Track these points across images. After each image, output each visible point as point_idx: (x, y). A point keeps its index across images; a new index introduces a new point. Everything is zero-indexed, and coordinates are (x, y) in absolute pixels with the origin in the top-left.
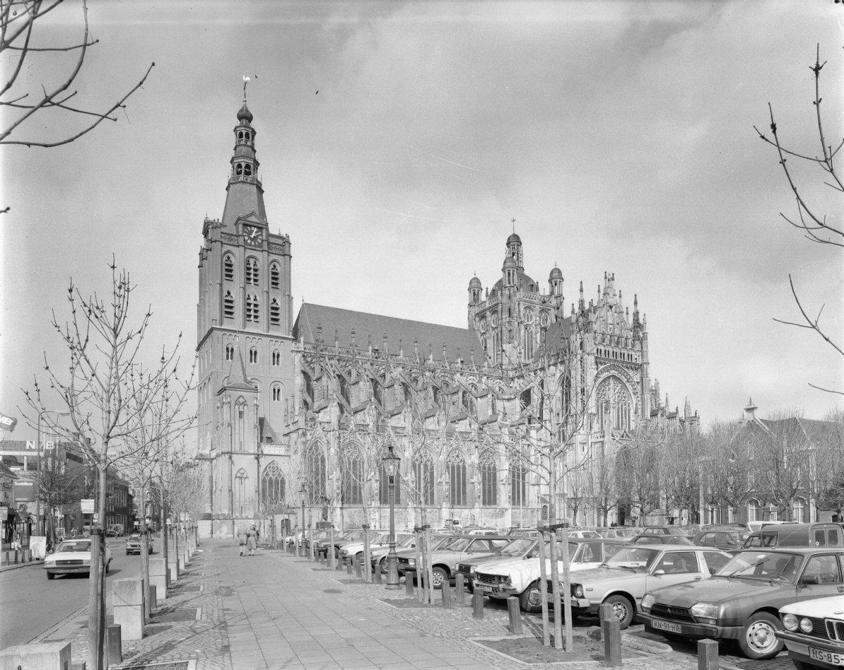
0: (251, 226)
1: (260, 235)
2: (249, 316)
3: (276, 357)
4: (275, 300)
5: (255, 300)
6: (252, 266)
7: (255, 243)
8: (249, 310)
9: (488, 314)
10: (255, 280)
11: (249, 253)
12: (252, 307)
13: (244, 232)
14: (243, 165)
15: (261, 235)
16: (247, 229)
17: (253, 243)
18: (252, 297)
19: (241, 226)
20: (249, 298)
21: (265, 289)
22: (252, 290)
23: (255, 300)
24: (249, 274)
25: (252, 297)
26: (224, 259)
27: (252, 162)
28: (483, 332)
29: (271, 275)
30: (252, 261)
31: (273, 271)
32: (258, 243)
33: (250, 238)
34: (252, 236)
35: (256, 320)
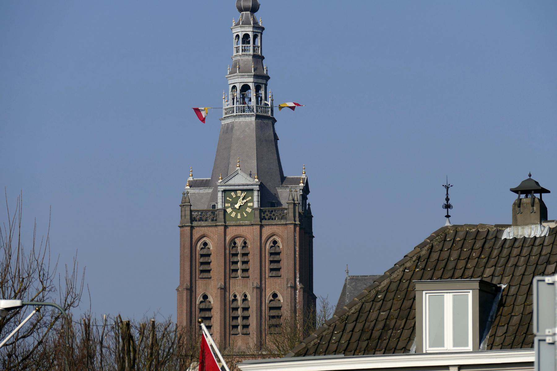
2: (236, 327)
5: (245, 299)
6: (239, 250)
7: (242, 215)
8: (236, 318)
10: (245, 271)
11: (231, 232)
12: (240, 312)
13: (225, 201)
15: (252, 201)
16: (231, 197)
17: (239, 217)
19: (220, 194)
20: (235, 300)
23: (245, 299)
25: (239, 298)
26: (198, 248)
29: (268, 258)
30: (239, 242)
32: (247, 213)
33: (234, 209)
34: (237, 206)
35: (245, 331)
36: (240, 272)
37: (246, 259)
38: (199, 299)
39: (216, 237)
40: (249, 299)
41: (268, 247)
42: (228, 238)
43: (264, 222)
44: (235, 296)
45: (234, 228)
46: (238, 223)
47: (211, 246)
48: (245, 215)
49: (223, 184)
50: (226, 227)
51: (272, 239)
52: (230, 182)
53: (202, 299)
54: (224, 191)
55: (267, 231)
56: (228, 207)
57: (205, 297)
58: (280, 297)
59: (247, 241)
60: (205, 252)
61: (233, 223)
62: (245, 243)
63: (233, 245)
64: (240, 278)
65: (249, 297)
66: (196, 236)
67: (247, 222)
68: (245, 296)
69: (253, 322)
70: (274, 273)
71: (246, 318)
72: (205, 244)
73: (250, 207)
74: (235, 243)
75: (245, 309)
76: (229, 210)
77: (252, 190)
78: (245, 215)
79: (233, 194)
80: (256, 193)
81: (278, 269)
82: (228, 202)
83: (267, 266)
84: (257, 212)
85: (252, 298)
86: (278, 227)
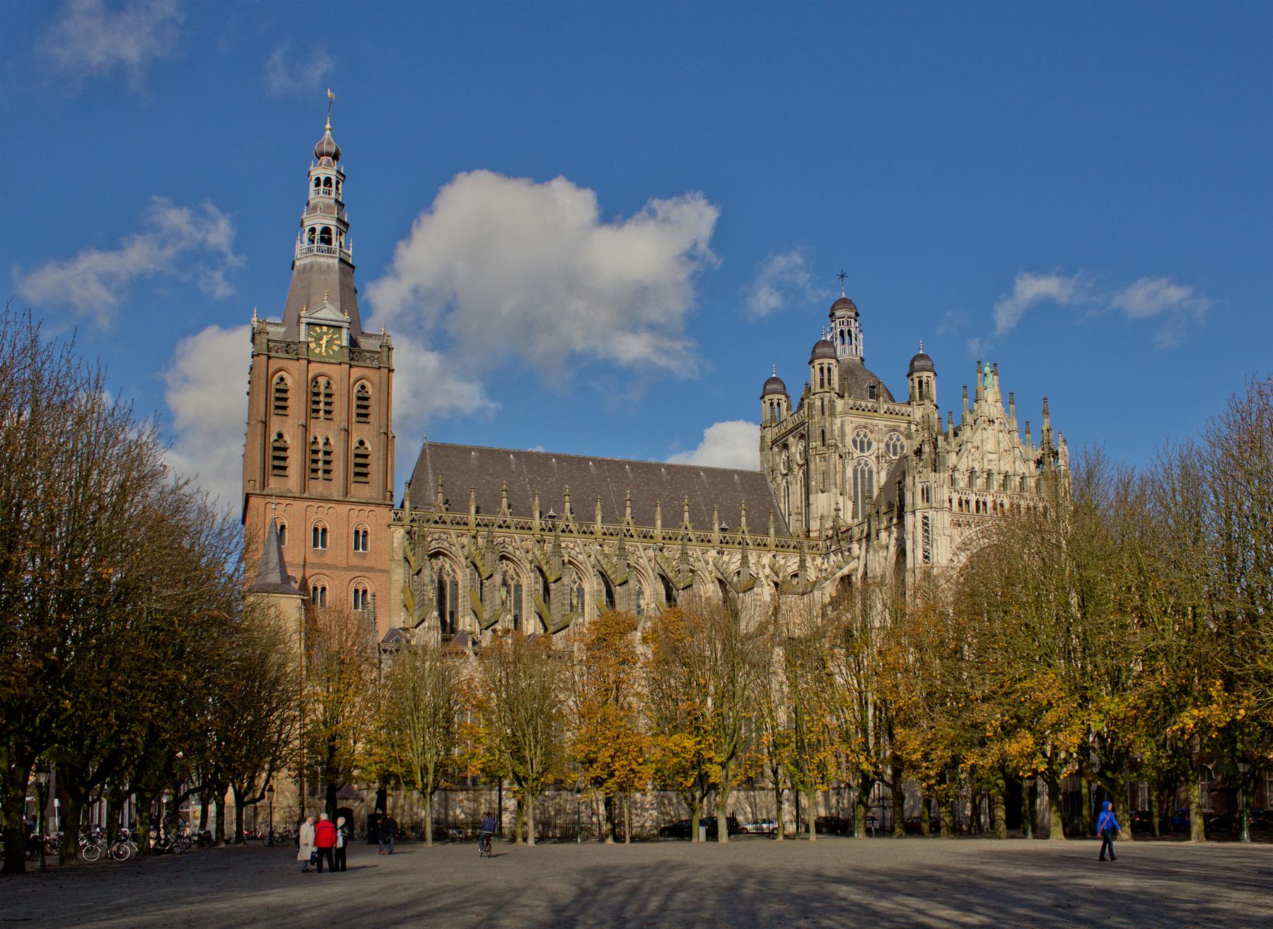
0: (321, 325)
1: (337, 339)
3: (360, 538)
4: (362, 443)
6: (322, 389)
9: (791, 439)
11: (315, 369)
12: (321, 455)
13: (309, 335)
14: (319, 229)
16: (315, 332)
18: (321, 441)
19: (303, 327)
20: (315, 442)
21: (344, 425)
22: (320, 430)
24: (317, 403)
25: (321, 441)
27: (334, 223)
28: (784, 472)
31: (360, 395)
32: (333, 350)
35: (327, 476)
36: (322, 413)
37: (329, 400)
38: (274, 437)
39: (296, 373)
40: (332, 443)
41: (355, 390)
42: (310, 375)
43: (353, 363)
44: (316, 438)
45: (319, 365)
46: (323, 360)
47: (289, 381)
48: (331, 353)
49: (307, 315)
50: (309, 362)
51: (360, 382)
52: (316, 315)
53: (276, 437)
54: (308, 324)
55: (356, 373)
56: (312, 342)
57: (280, 436)
58: (368, 444)
59: (332, 382)
60: (281, 387)
61: (317, 359)
62: (329, 383)
63: (314, 384)
64: (322, 419)
65: (332, 442)
66: (272, 369)
67: (333, 361)
68: (328, 439)
69: (338, 467)
70: (362, 419)
71: (327, 462)
72: (282, 379)
73: (337, 345)
74: (317, 382)
75: (327, 453)
76: (312, 346)
77: (340, 327)
78: (331, 353)
79: (317, 328)
80: (345, 331)
81: (366, 416)
82: (312, 336)
83: (354, 410)
84: (346, 351)
85: (336, 442)
86: (368, 370)
